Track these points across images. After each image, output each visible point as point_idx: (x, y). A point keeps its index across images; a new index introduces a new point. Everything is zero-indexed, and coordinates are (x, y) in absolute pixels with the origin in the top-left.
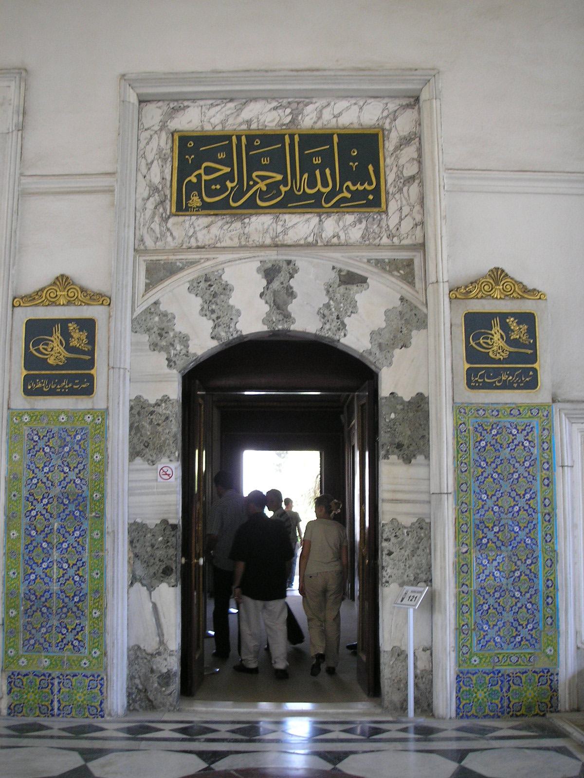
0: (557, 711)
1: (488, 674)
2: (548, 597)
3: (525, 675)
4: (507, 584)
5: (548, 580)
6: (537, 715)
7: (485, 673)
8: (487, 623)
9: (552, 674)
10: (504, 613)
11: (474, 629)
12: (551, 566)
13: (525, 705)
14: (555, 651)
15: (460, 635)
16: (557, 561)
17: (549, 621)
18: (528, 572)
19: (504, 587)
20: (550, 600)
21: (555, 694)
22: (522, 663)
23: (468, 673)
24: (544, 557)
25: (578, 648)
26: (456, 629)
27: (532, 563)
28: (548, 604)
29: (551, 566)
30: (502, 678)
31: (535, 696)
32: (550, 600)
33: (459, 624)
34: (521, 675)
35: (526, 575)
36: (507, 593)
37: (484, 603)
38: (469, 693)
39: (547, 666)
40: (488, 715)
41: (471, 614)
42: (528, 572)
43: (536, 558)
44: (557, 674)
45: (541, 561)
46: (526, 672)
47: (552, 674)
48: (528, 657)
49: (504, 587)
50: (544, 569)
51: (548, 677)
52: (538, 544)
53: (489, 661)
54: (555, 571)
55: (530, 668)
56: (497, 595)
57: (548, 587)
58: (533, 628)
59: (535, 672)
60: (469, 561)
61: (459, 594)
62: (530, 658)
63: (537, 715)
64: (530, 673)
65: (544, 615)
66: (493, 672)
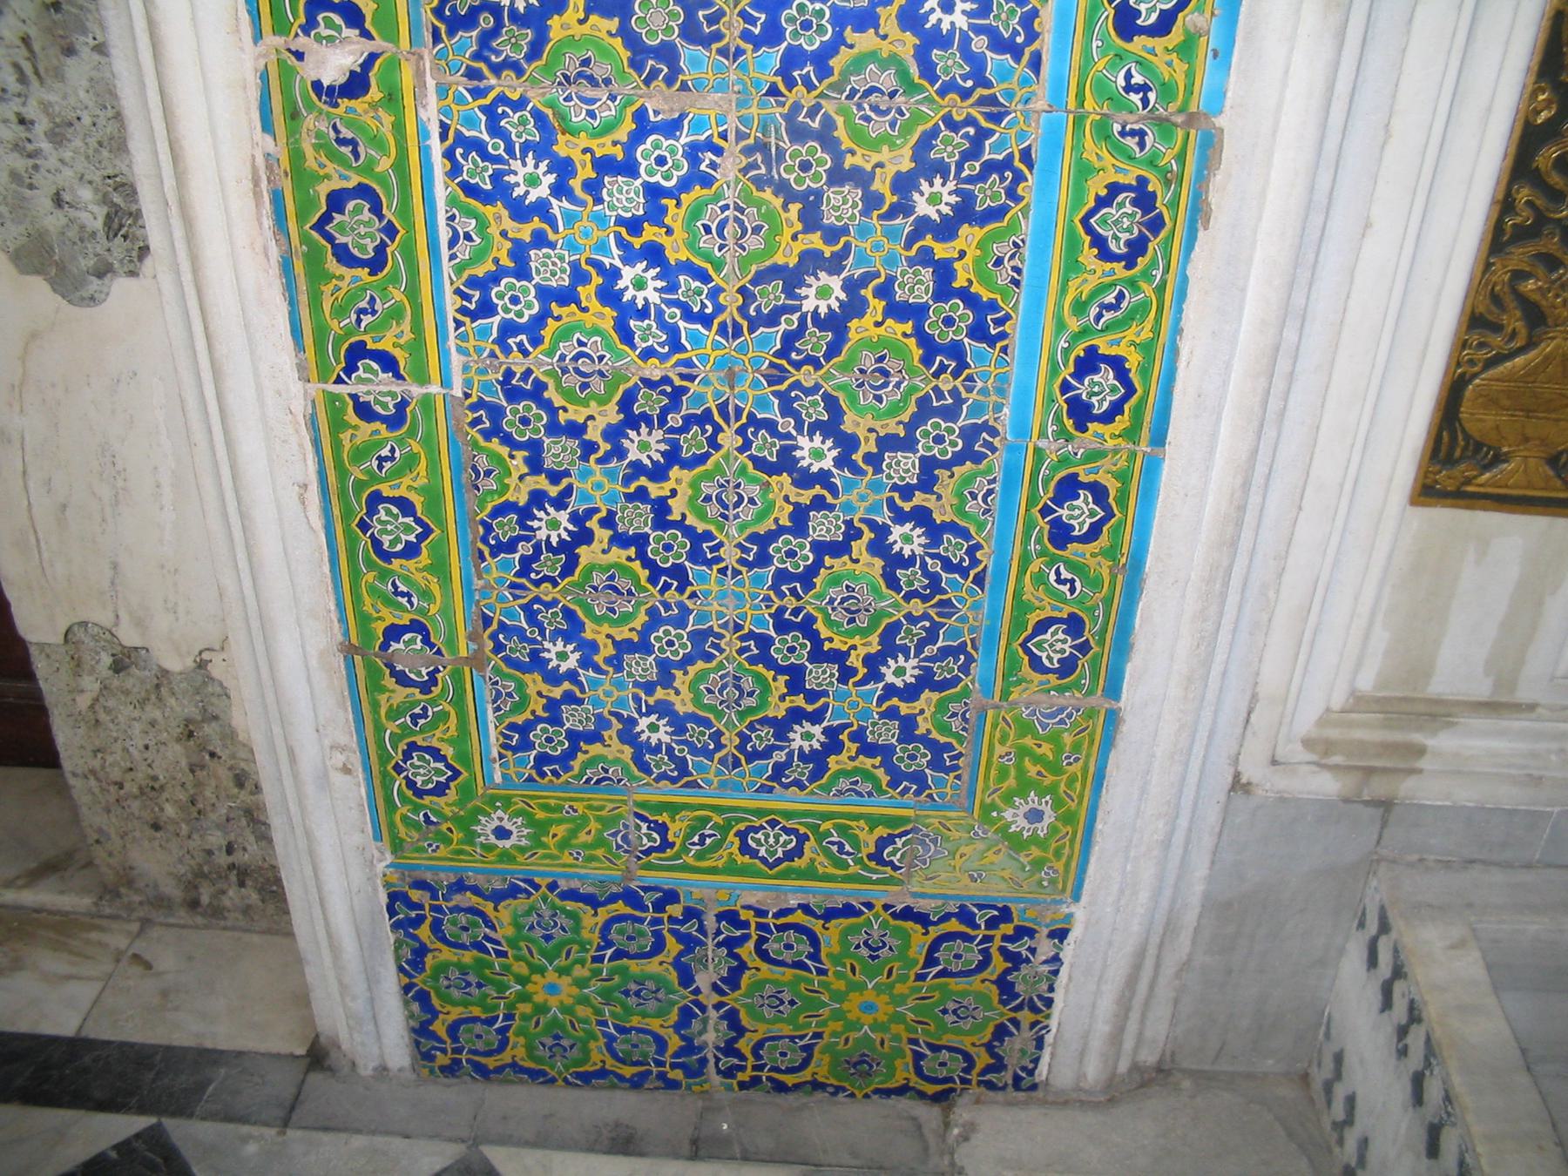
0: (1024, 1083)
1: (592, 901)
2: (1068, 488)
3: (838, 924)
4: (732, 379)
5: (1088, 363)
6: (902, 1090)
7: (572, 895)
8: (572, 629)
9: (1023, 932)
10: (705, 580)
11: (477, 661)
12: (1137, 248)
13: (829, 1049)
14: (1069, 818)
15: (375, 686)
16: (1200, 212)
17: (1056, 644)
18: (917, 286)
19: (706, 393)
20: (1079, 513)
21: (1025, 1016)
22: (824, 866)
23: (460, 886)
24: (1084, 171)
25: (1239, 785)
26: (349, 650)
27: (965, 212)
28: (1061, 535)
29: (1137, 248)
30: (691, 928)
31: (898, 1018)
32: (1079, 513)
33: (364, 620)
34: (816, 925)
35: (897, 311)
36: (729, 439)
37: (538, 498)
38: (472, 981)
39: (997, 890)
40: (603, 1073)
41: (439, 568)
42: (917, 286)
43: (1011, 170)
44: (1060, 934)
45: (1047, 208)
46: (848, 911)
47: (1023, 932)
48: (869, 841)
49: (706, 393)
50: (1072, 265)
51: (998, 942)
52: (1047, 44)
53: (600, 842)
54: (1171, 297)
55: (880, 894)
56: (644, 446)
57: (1081, 413)
58: (926, 681)
59: (907, 914)
60: (384, 164)
61: (337, 425)
62: (883, 843)
63: (902, 1090)
64: (876, 922)
65: (1021, 606)
66: (631, 898)
